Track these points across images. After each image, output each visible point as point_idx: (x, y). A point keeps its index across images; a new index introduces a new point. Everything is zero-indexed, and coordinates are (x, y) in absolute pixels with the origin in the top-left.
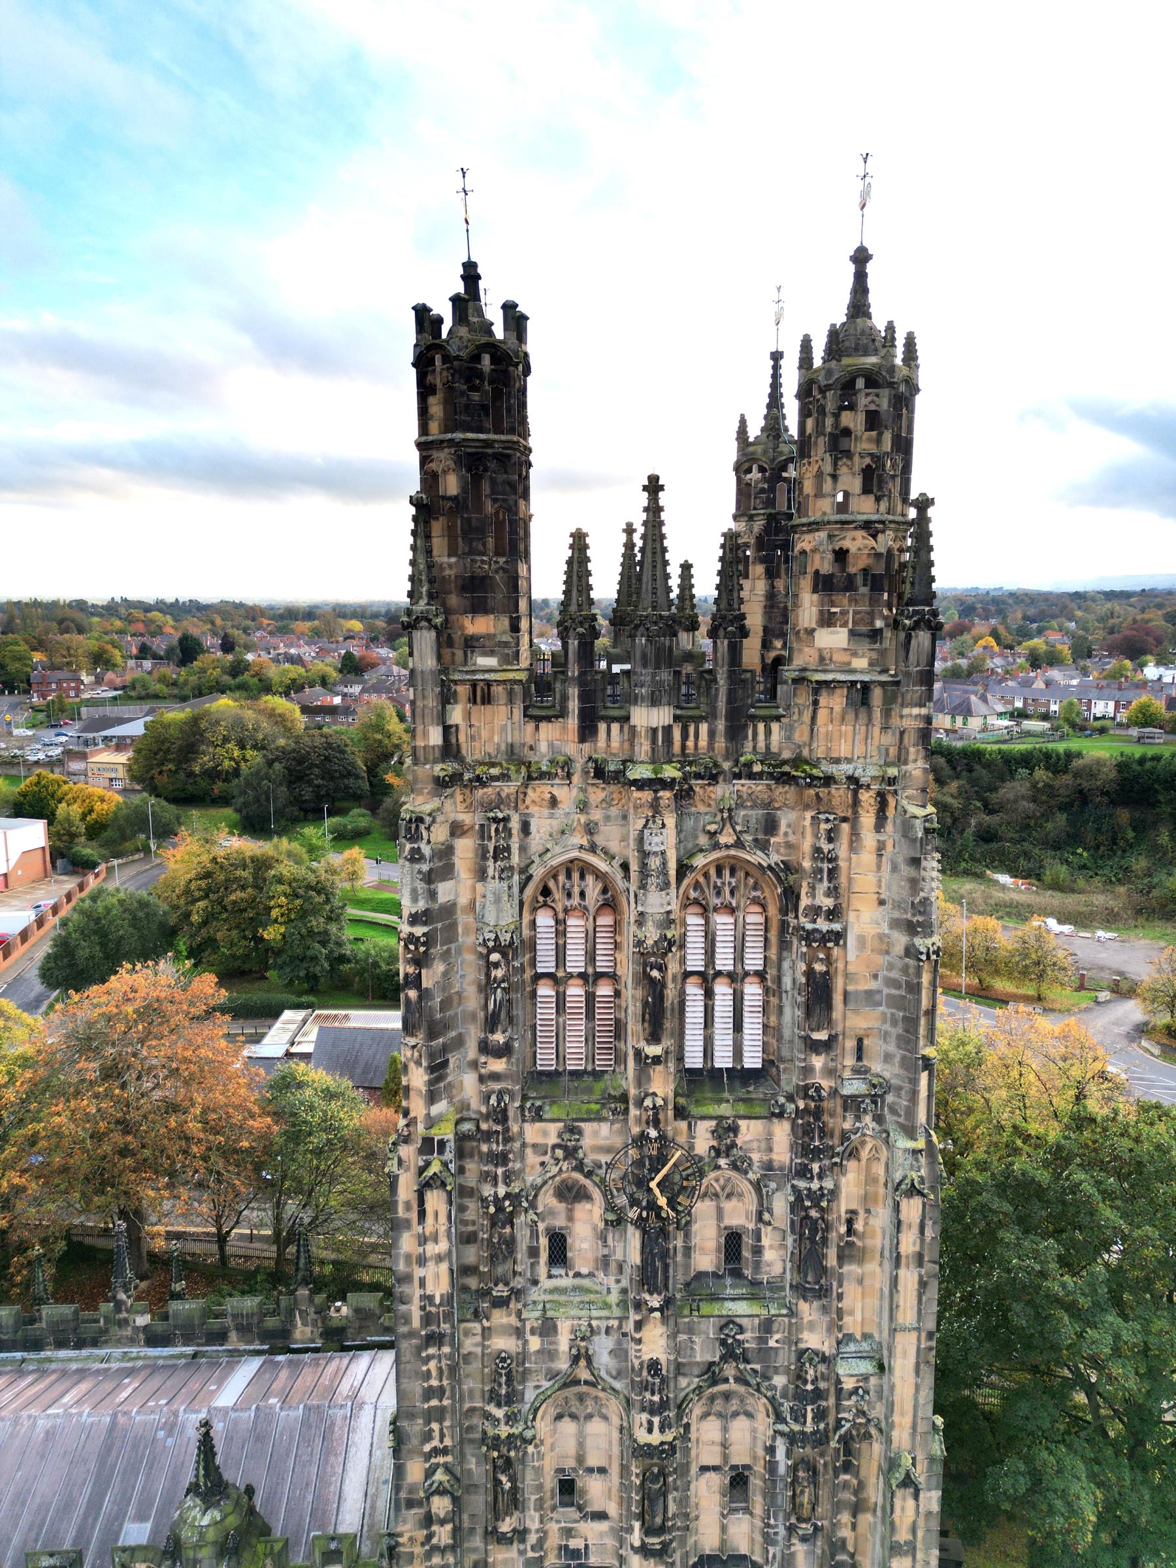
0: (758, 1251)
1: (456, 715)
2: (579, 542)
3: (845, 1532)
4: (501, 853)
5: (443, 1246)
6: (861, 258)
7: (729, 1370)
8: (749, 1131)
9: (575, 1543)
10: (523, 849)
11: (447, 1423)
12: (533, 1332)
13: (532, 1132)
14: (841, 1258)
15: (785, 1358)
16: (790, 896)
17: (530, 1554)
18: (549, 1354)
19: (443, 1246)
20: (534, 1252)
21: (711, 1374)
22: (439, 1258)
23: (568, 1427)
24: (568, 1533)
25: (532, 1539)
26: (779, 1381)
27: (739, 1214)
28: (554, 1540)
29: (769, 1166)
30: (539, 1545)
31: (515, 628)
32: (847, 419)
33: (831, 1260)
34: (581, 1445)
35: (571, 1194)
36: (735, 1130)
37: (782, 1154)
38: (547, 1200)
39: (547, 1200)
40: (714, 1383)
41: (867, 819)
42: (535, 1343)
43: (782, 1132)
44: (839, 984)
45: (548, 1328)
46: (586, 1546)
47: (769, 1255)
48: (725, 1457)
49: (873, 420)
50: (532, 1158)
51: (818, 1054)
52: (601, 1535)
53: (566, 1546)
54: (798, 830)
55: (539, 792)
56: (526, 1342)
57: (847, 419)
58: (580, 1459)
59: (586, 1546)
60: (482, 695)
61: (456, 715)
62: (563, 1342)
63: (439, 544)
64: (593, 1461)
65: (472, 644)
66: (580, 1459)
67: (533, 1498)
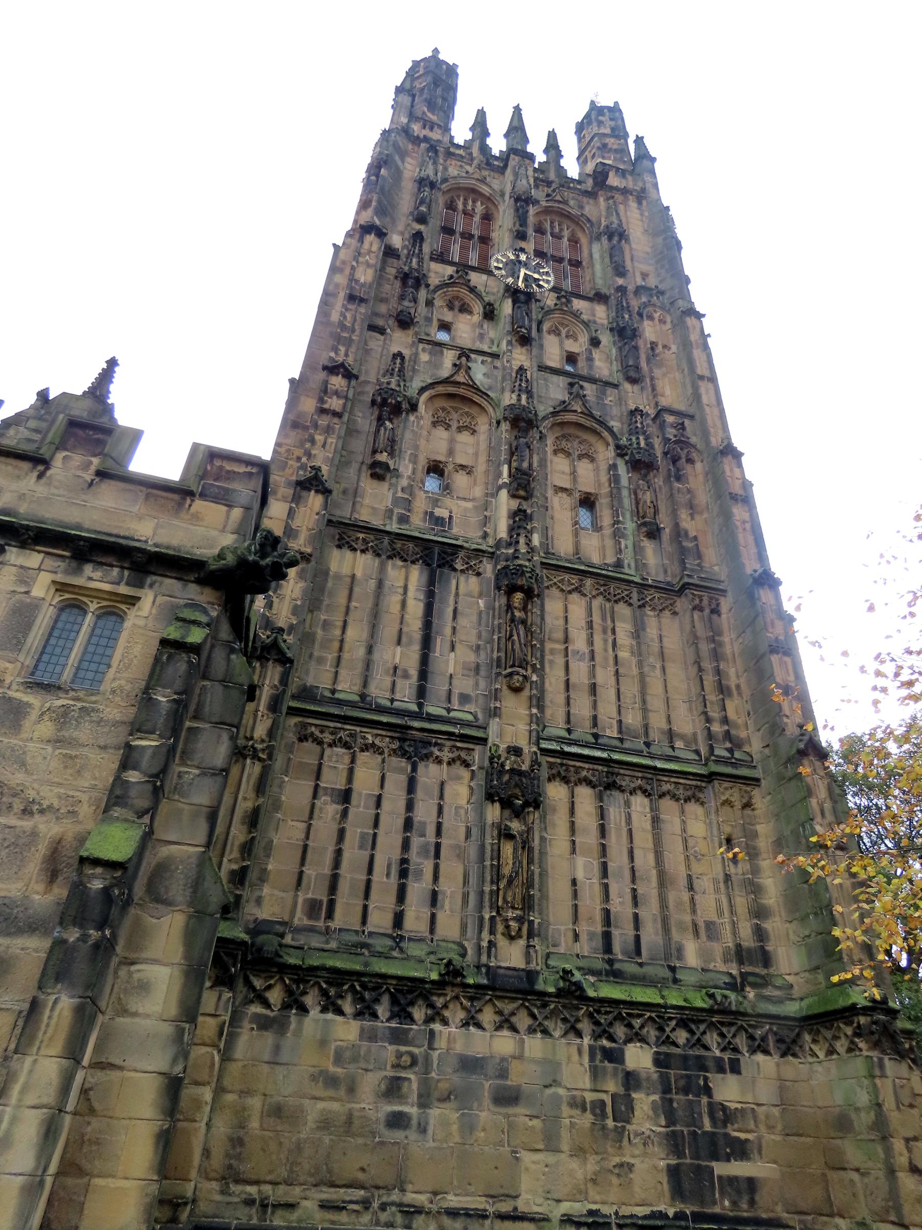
2: (481, 116)
9: (440, 512)
11: (353, 349)
12: (424, 350)
17: (400, 494)
22: (368, 265)
23: (441, 433)
28: (420, 504)
34: (452, 441)
40: (565, 410)
42: (424, 357)
46: (451, 517)
48: (575, 480)
52: (466, 509)
53: (432, 513)
56: (416, 354)
57: (601, 118)
58: (451, 452)
59: (451, 517)
64: (460, 460)
66: (451, 452)
67: (409, 452)
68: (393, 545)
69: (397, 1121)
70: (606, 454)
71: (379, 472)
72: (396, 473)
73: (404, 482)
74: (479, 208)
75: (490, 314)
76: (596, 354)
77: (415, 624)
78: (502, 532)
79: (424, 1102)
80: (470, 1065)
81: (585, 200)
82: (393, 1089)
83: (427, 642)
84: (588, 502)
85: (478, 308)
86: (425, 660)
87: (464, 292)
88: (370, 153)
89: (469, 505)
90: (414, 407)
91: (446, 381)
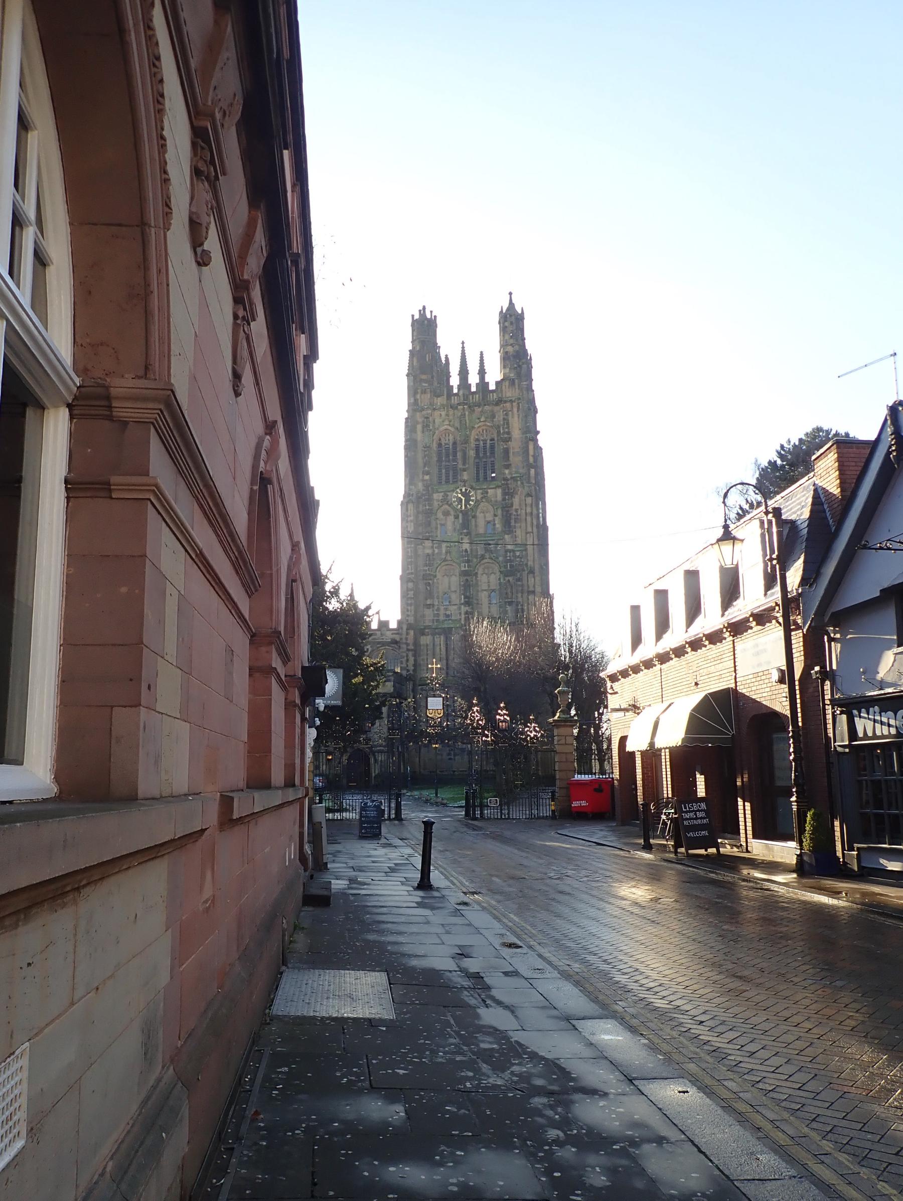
0: (494, 525)
1: (418, 396)
3: (520, 600)
4: (428, 426)
5: (412, 518)
6: (510, 294)
7: (487, 555)
8: (491, 492)
9: (448, 613)
10: (434, 426)
13: (435, 496)
14: (515, 522)
15: (502, 552)
16: (499, 432)
18: (440, 553)
19: (412, 518)
20: (437, 528)
21: (483, 557)
22: (411, 521)
23: (446, 579)
24: (446, 609)
25: (436, 608)
26: (501, 559)
27: (489, 517)
28: (442, 612)
29: (496, 501)
30: (438, 610)
31: (432, 377)
32: (506, 324)
33: (513, 524)
35: (446, 514)
36: (487, 493)
37: (499, 497)
38: (440, 515)
39: (440, 515)
41: (515, 410)
42: (436, 551)
43: (499, 491)
44: (511, 451)
45: (440, 547)
47: (497, 526)
49: (512, 323)
50: (436, 504)
51: (507, 468)
54: (499, 417)
55: (437, 413)
57: (506, 324)
60: (424, 392)
61: (418, 396)
62: (444, 551)
63: (415, 360)
64: (453, 589)
65: (421, 380)
68: (435, 632)
69: (450, 759)
70: (498, 574)
71: (429, 606)
72: (433, 605)
73: (436, 608)
74: (451, 437)
75: (456, 517)
76: (497, 518)
77: (444, 656)
78: (463, 623)
79: (455, 755)
80: (463, 750)
81: (496, 408)
82: (449, 754)
83: (447, 660)
84: (493, 591)
85: (452, 513)
86: (447, 664)
87: (447, 507)
88: (403, 439)
89: (455, 607)
90: (435, 576)
91: (445, 560)
